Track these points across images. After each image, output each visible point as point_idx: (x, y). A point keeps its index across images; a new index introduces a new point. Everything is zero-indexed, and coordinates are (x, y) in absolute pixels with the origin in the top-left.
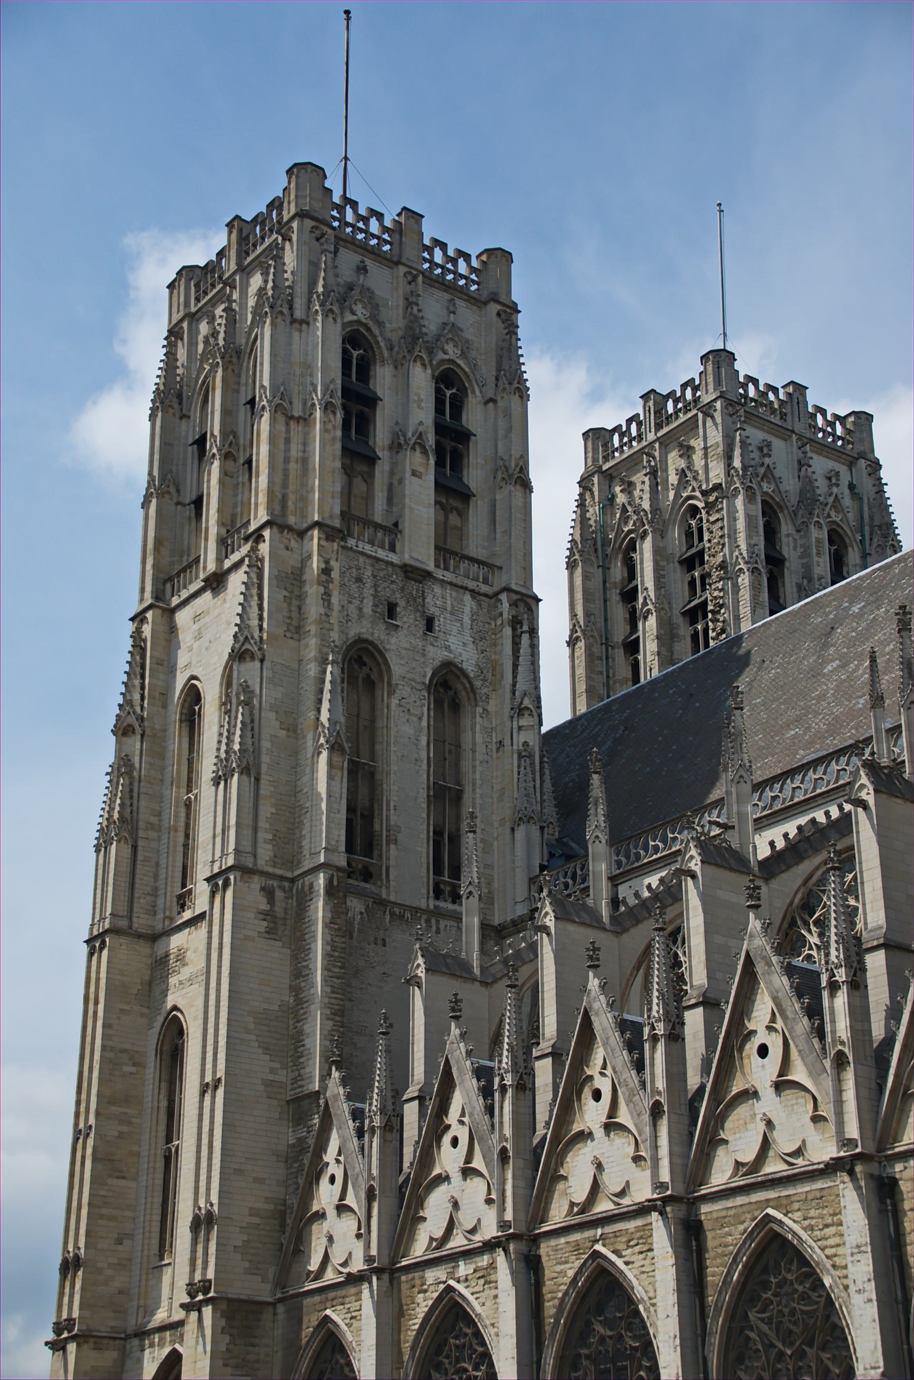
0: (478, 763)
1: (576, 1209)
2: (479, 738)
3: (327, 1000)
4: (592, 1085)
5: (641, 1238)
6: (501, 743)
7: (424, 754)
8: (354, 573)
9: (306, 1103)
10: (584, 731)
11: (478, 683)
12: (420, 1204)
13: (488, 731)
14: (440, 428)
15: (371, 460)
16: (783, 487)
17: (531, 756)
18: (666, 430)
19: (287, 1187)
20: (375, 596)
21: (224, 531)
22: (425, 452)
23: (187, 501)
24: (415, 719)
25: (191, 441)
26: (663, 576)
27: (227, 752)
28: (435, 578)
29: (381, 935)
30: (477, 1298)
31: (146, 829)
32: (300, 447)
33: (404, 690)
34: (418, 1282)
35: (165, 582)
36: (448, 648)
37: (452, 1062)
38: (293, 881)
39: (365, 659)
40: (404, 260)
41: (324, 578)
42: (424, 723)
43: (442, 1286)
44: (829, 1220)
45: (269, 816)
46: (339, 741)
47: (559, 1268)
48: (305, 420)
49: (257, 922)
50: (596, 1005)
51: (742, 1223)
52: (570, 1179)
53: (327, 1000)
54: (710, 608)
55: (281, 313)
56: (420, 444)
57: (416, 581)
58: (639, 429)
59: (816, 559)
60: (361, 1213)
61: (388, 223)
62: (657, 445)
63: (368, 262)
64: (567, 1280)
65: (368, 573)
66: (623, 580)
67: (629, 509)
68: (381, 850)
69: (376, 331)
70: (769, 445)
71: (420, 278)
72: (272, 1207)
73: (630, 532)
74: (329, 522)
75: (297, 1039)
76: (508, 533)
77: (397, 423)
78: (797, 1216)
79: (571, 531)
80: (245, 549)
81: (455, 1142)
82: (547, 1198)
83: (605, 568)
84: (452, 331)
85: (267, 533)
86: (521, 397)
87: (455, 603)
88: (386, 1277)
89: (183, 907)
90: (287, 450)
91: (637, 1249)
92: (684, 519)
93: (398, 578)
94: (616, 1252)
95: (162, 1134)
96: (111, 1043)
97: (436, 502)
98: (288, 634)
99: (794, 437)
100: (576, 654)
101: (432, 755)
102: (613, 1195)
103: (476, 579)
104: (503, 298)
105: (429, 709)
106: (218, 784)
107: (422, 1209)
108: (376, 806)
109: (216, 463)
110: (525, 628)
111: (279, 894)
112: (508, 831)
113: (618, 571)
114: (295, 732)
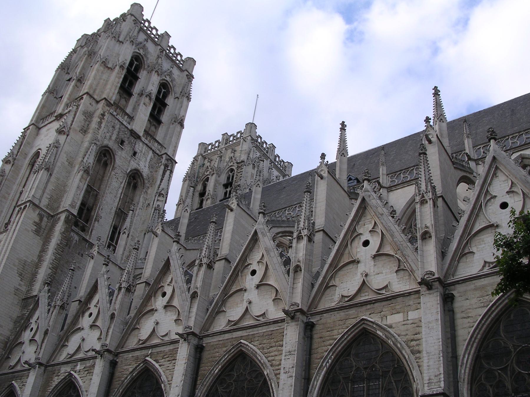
0: (138, 208)
1: (141, 342)
2: (142, 199)
3: (52, 261)
4: (163, 290)
5: (171, 354)
7: (119, 195)
11: (146, 182)
12: (67, 340)
13: (146, 199)
15: (130, 95)
20: (118, 135)
22: (150, 99)
24: (119, 182)
26: (216, 189)
28: (141, 140)
30: (82, 380)
35: (41, 119)
36: (139, 165)
38: (52, 216)
39: (107, 155)
41: (101, 116)
42: (122, 185)
44: (274, 344)
45: (51, 189)
46: (88, 170)
47: (125, 367)
48: (111, 69)
49: (32, 225)
51: (226, 347)
52: (141, 330)
53: (52, 261)
56: (149, 96)
57: (134, 138)
60: (39, 344)
62: (224, 149)
64: (128, 373)
65: (118, 126)
66: (201, 190)
68: (91, 222)
75: (34, 275)
77: (143, 87)
78: (255, 343)
79: (187, 170)
81: (91, 315)
82: (127, 338)
84: (170, 74)
85: (85, 97)
86: (188, 100)
87: (146, 152)
88: (43, 368)
92: (228, 172)
93: (129, 134)
97: (149, 120)
98: (81, 131)
100: (179, 209)
101: (122, 197)
102: (161, 336)
105: (125, 182)
106: (35, 173)
107: (67, 342)
109: (74, 82)
111: (45, 219)
112: (143, 234)
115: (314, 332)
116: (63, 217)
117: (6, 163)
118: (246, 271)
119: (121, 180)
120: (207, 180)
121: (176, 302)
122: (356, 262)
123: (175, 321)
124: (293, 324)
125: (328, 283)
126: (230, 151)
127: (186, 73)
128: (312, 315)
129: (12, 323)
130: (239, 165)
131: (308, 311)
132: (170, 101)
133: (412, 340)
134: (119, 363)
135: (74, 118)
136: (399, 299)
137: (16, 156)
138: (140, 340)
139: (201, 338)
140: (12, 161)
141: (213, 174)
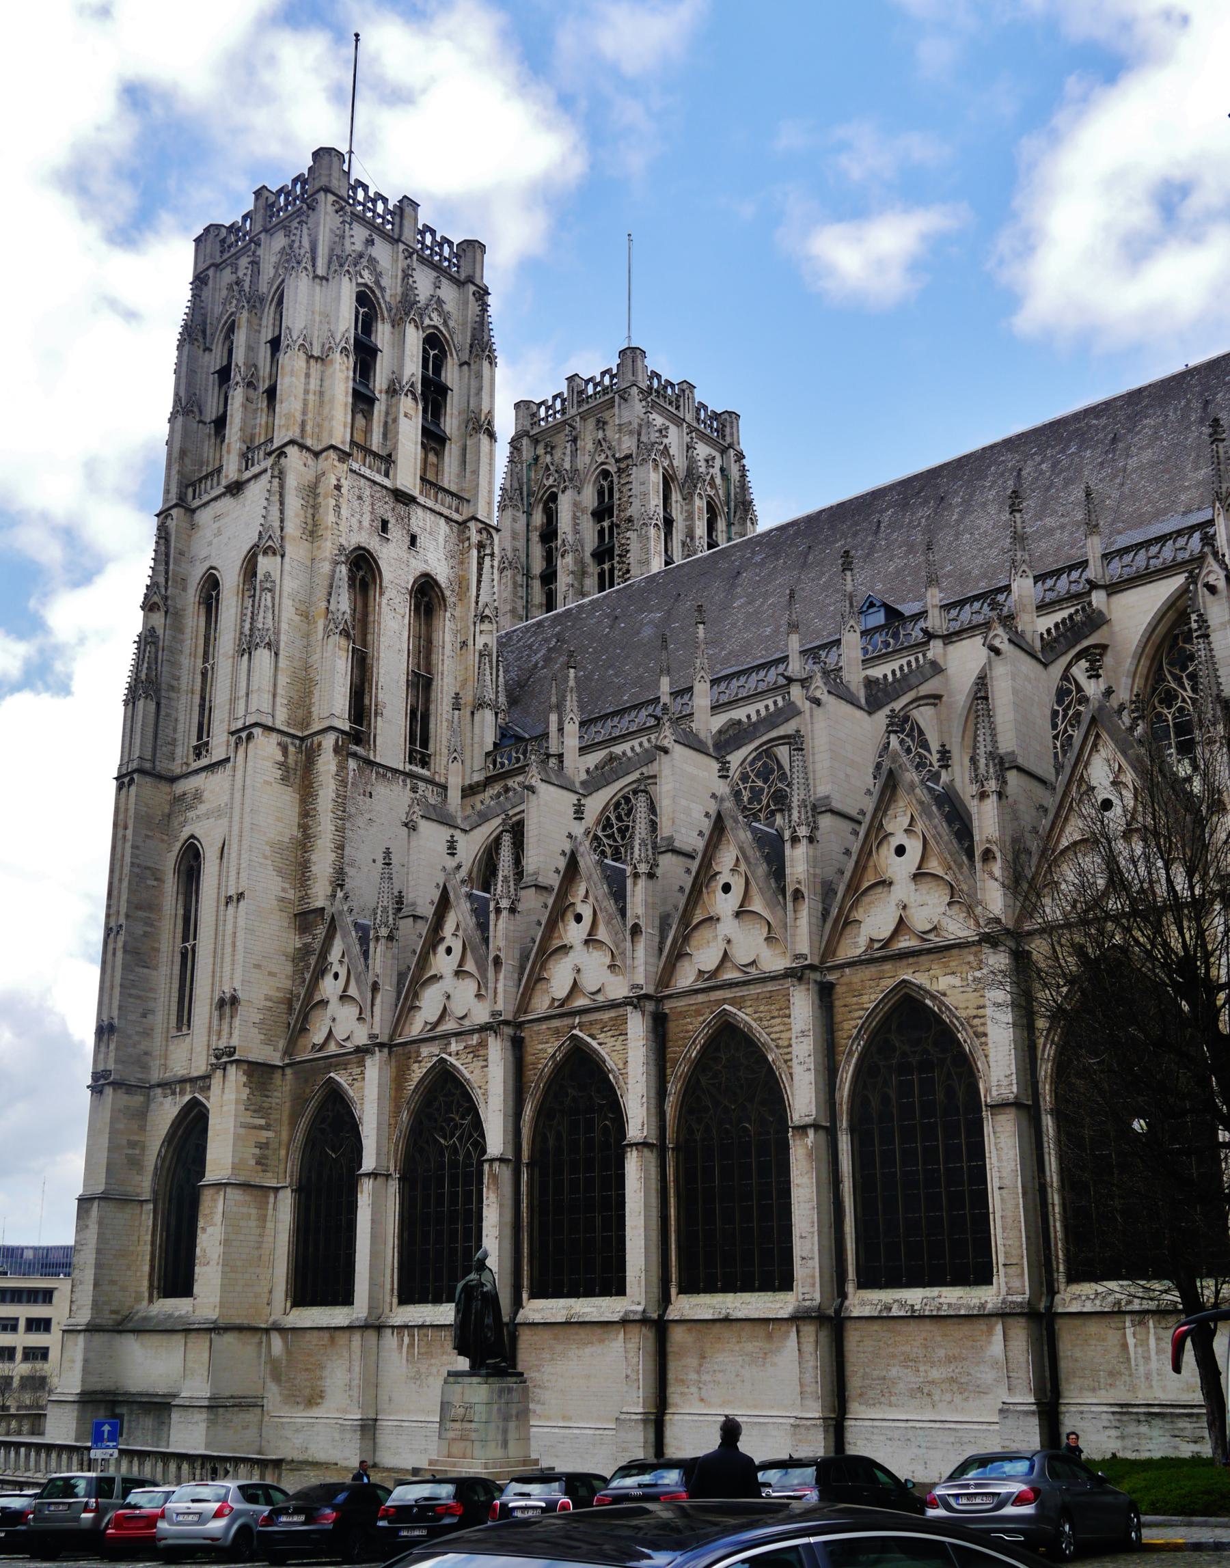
1: (556, 1004)
6: (464, 644)
8: (357, 493)
9: (311, 917)
10: (518, 641)
14: (425, 380)
16: (675, 463)
17: (490, 655)
18: (586, 407)
19: (294, 981)
21: (244, 448)
22: (415, 399)
23: (208, 420)
25: (212, 370)
27: (251, 630)
28: (419, 504)
29: (369, 789)
31: (168, 690)
32: (319, 382)
33: (390, 593)
34: (414, 1055)
35: (187, 486)
36: (426, 562)
37: (450, 889)
38: (302, 739)
40: (403, 239)
41: (336, 492)
42: (406, 621)
43: (435, 1059)
44: (776, 1014)
47: (540, 1047)
48: (322, 360)
50: (582, 849)
54: (617, 552)
55: (306, 268)
57: (405, 504)
58: (563, 404)
59: (697, 522)
61: (391, 207)
62: (578, 419)
63: (374, 236)
65: (367, 492)
67: (552, 468)
69: (379, 295)
70: (667, 428)
71: (415, 256)
72: (282, 995)
73: (551, 486)
74: (340, 446)
76: (476, 472)
77: (393, 373)
78: (749, 1010)
80: (270, 461)
83: (529, 514)
86: (491, 363)
88: (386, 1050)
89: (198, 756)
90: (307, 383)
91: (610, 1033)
93: (390, 500)
94: (591, 1036)
95: (179, 935)
96: (138, 861)
97: (422, 443)
99: (685, 425)
103: (450, 507)
104: (478, 281)
108: (367, 685)
110: (488, 551)
111: (291, 749)
112: (468, 714)
113: (538, 518)
114: (307, 617)
115: (835, 997)
116: (329, 741)
117: (151, 610)
118: (713, 884)
119: (402, 612)
120: (553, 498)
121: (602, 934)
122: (886, 884)
123: (609, 967)
124: (803, 987)
125: (847, 917)
126: (591, 423)
127: (472, 288)
128: (830, 969)
129: (290, 964)
130: (623, 466)
131: (822, 963)
132: (451, 375)
133: (975, 1017)
134: (527, 1040)
135: (282, 512)
136: (955, 952)
137: (166, 589)
138: (554, 999)
139: (659, 1000)
140: (161, 604)
141: (565, 488)
